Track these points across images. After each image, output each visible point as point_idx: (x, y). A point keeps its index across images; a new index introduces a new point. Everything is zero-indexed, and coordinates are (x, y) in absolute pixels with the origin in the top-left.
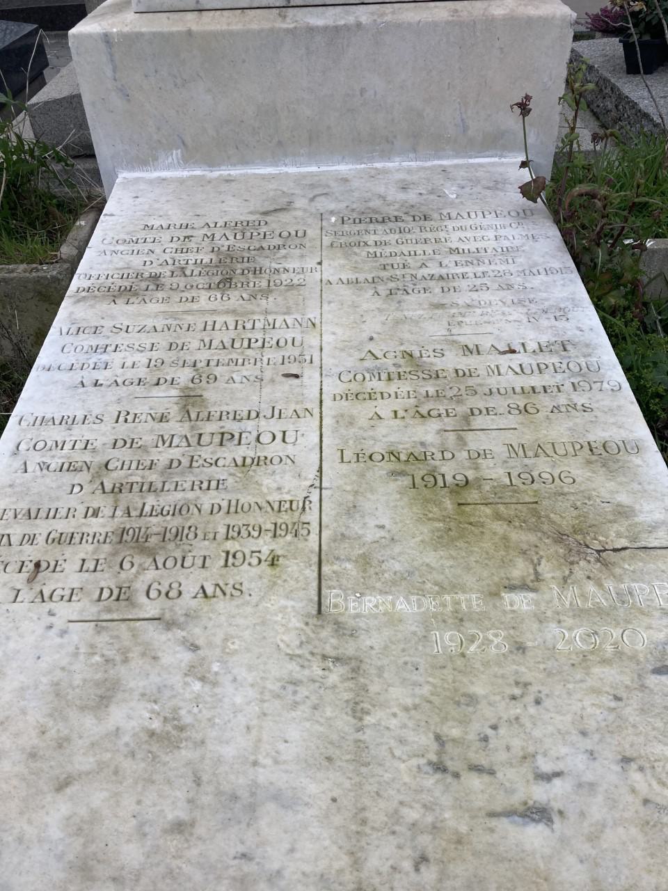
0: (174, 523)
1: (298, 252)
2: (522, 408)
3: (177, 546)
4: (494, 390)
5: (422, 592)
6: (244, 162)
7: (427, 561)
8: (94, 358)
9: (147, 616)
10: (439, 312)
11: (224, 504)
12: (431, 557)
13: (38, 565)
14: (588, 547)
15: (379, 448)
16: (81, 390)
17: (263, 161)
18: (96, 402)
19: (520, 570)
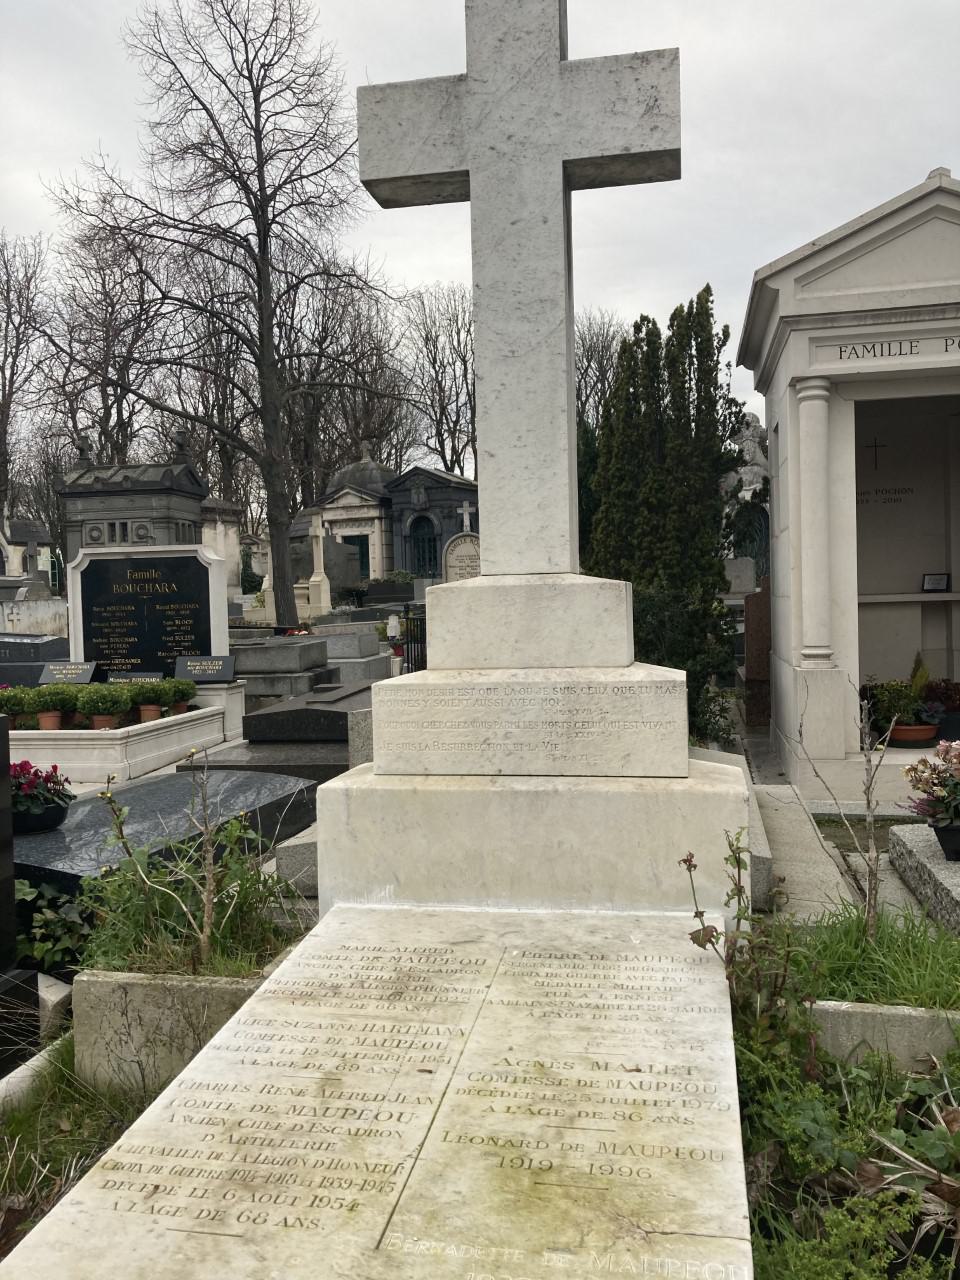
0: (278, 1170)
1: (472, 976)
2: (627, 1116)
3: (276, 1187)
4: (608, 1099)
5: (472, 1243)
6: (449, 900)
7: (488, 1221)
8: (260, 1043)
9: (234, 1233)
10: (582, 1034)
11: (328, 1162)
12: (492, 1220)
13: (157, 1187)
14: (639, 1227)
15: (483, 1133)
16: (241, 1066)
17: (468, 901)
18: (248, 1076)
19: (569, 1236)
